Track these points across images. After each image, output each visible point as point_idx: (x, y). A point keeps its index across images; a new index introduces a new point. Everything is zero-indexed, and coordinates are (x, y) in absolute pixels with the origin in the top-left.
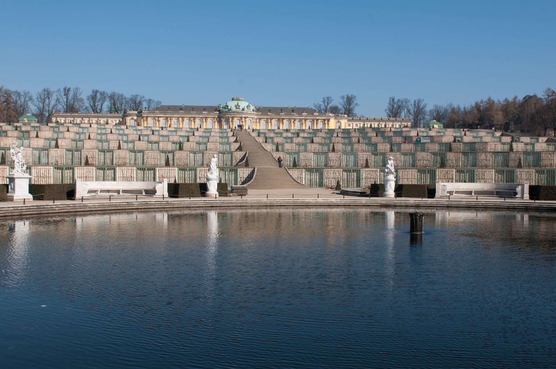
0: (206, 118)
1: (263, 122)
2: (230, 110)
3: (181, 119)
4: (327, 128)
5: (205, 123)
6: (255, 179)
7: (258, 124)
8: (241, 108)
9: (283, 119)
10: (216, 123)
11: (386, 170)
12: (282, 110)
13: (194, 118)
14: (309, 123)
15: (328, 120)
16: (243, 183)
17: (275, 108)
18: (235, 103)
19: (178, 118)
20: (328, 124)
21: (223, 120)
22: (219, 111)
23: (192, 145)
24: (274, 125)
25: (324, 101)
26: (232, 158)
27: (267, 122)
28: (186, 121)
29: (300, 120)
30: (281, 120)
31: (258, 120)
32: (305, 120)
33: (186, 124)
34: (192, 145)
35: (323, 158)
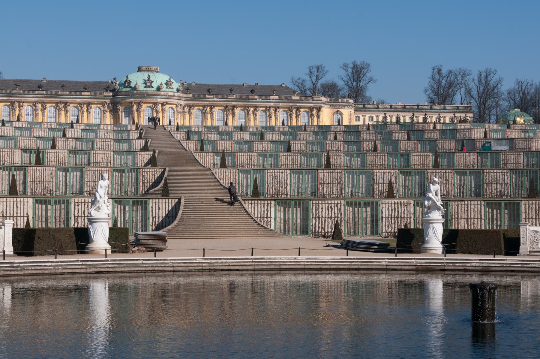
0: (89, 104)
1: (196, 112)
2: (135, 88)
3: (39, 106)
4: (315, 123)
5: (85, 114)
6: (181, 219)
7: (187, 116)
8: (155, 85)
9: (234, 107)
10: (108, 114)
11: (426, 203)
12: (231, 90)
13: (66, 103)
14: (282, 115)
15: (319, 109)
16: (158, 228)
17: (219, 86)
18: (144, 76)
19: (35, 104)
20: (318, 116)
21: (121, 108)
22: (113, 91)
23: (61, 156)
24: (216, 118)
25: (310, 74)
26: (137, 179)
27: (204, 113)
28: (50, 109)
29: (267, 109)
30: (229, 109)
31: (187, 109)
32: (276, 109)
33: (49, 116)
34: (61, 156)
35: (308, 179)
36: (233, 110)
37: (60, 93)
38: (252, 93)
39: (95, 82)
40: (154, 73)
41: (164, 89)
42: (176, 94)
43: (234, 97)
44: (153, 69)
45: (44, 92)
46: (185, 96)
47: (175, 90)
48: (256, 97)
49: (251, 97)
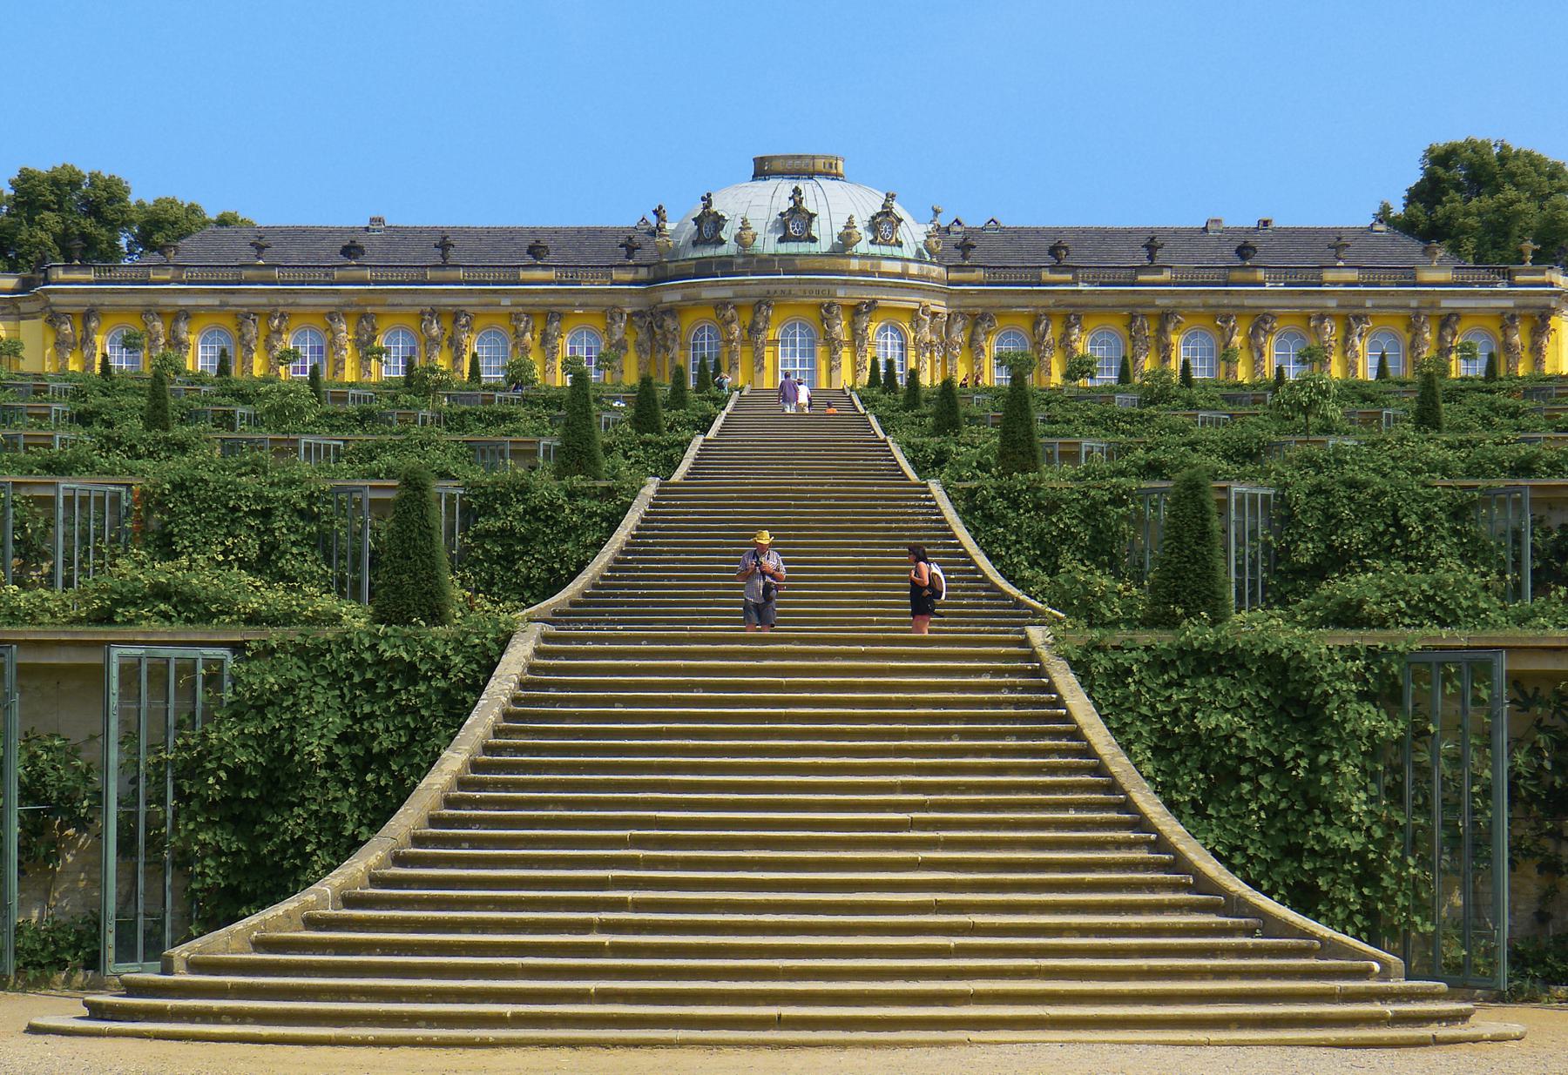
18: (778, 194)
36: (1162, 331)
37: (429, 274)
38: (1244, 257)
39: (579, 231)
40: (823, 182)
41: (863, 247)
42: (914, 269)
43: (1166, 275)
44: (820, 165)
45: (368, 273)
46: (953, 276)
47: (908, 252)
48: (1260, 275)
49: (1237, 275)
